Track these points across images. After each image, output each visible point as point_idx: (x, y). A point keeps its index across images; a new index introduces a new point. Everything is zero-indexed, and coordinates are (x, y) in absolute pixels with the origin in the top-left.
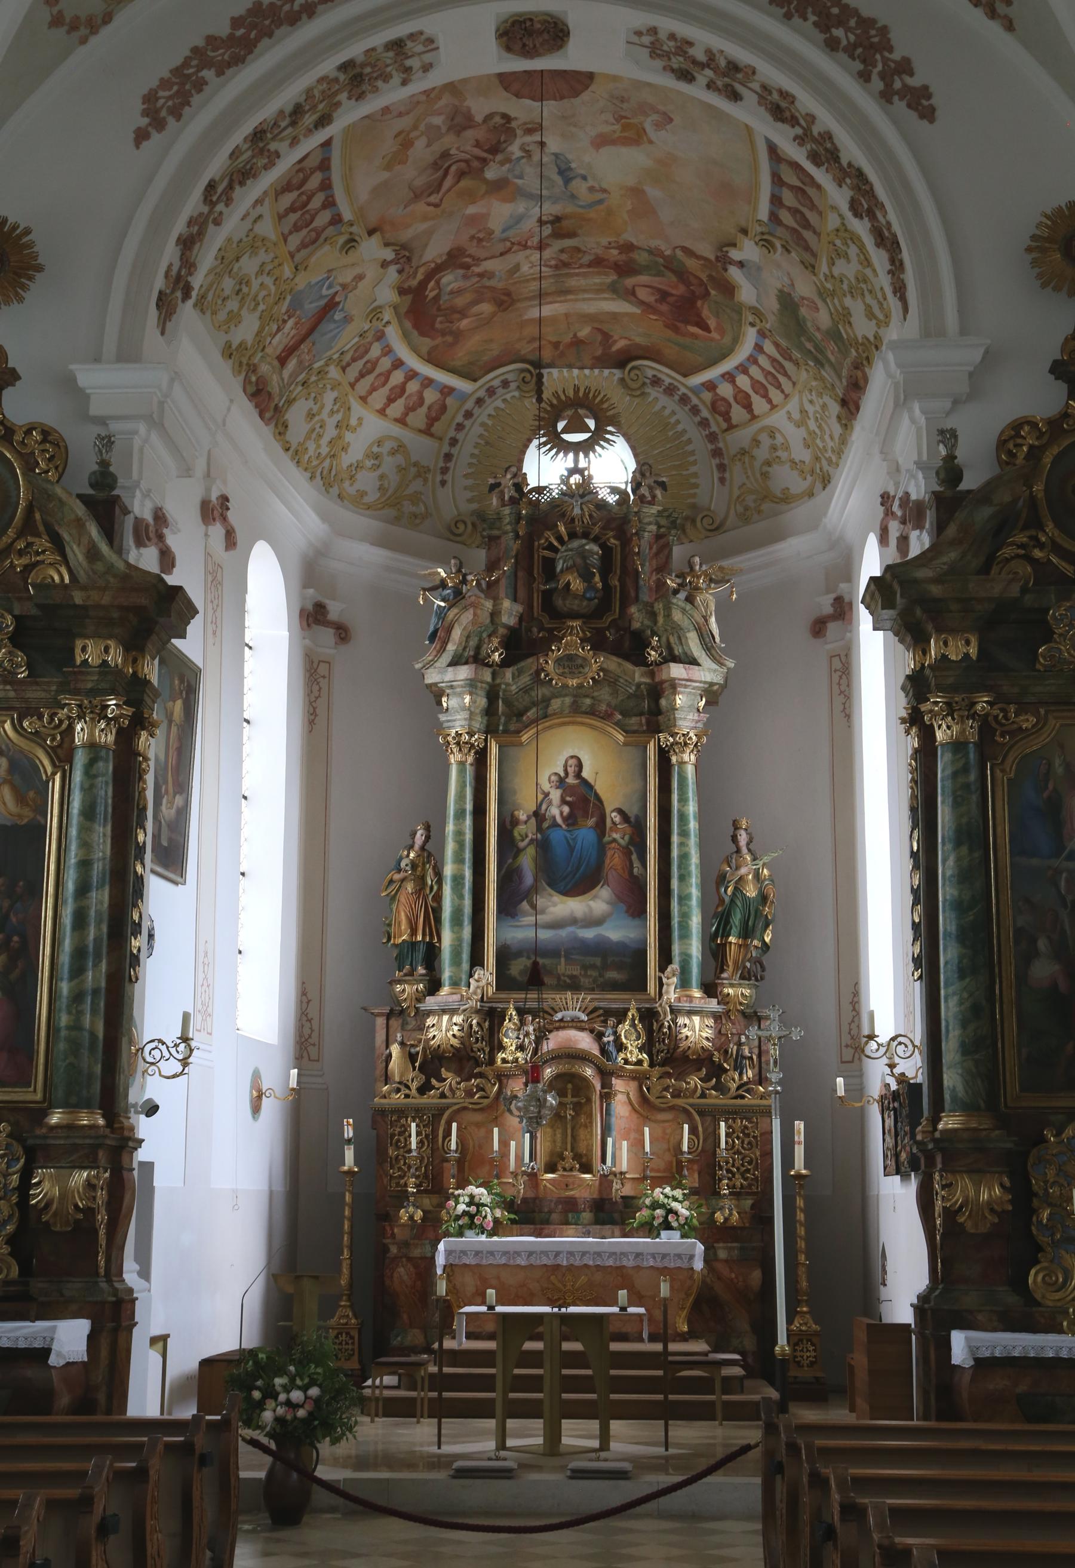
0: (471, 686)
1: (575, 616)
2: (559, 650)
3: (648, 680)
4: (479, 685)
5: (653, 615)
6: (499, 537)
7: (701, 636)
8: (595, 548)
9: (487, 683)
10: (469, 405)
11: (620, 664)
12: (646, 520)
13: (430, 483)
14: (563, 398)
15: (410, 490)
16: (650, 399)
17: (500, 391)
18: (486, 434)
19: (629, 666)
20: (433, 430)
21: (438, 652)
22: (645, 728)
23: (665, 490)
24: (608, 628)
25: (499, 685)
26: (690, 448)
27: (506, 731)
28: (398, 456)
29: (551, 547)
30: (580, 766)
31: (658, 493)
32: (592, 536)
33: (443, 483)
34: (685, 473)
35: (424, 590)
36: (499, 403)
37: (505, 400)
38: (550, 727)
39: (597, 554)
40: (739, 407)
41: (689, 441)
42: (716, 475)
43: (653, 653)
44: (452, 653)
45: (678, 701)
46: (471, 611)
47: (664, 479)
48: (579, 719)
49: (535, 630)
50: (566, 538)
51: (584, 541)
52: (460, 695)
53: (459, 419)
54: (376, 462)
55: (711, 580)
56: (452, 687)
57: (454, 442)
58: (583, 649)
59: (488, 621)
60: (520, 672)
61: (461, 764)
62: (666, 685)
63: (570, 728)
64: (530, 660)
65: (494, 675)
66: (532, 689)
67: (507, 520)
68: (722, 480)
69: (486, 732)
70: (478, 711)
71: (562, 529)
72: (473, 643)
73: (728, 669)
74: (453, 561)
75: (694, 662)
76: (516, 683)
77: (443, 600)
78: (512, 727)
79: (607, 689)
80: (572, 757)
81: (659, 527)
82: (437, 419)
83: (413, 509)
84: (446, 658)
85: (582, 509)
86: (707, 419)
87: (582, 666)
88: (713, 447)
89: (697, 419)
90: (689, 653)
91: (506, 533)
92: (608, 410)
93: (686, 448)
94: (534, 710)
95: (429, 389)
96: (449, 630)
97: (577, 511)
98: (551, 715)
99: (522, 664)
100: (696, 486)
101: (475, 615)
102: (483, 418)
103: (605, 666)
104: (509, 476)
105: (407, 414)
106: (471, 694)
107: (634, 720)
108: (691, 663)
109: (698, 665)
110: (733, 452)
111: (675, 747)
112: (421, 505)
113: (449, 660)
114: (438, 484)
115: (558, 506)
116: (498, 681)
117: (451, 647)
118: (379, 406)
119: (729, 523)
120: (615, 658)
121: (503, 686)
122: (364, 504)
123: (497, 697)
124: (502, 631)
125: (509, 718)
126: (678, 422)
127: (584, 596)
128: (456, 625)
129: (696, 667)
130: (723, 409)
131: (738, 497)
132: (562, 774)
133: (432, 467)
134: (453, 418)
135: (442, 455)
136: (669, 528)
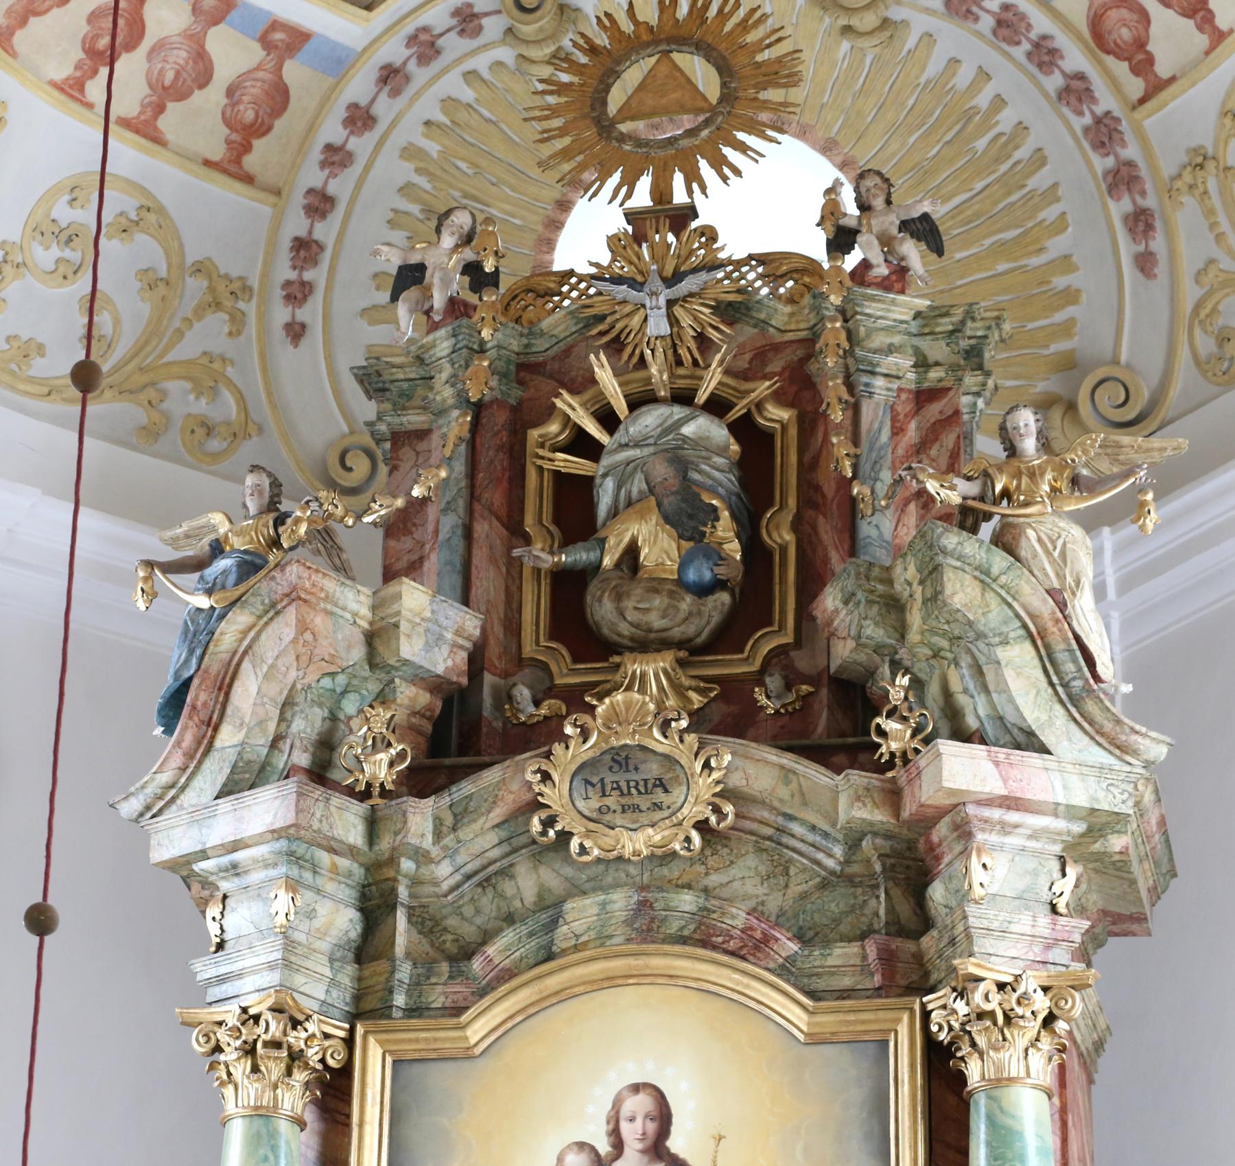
0: (292, 857)
1: (646, 644)
2: (585, 734)
3: (878, 816)
4: (324, 858)
5: (894, 607)
6: (422, 434)
7: (1048, 659)
8: (715, 431)
9: (352, 852)
10: (359, 87)
11: (786, 772)
12: (879, 340)
13: (252, 328)
14: (627, 26)
15: (188, 349)
16: (911, 43)
17: (453, 45)
18: (422, 182)
19: (814, 774)
20: (251, 162)
21: (190, 756)
22: (877, 980)
23: (938, 249)
24: (758, 678)
25: (392, 861)
26: (1042, 180)
27: (415, 1011)
28: (141, 238)
29: (582, 445)
30: (663, 1117)
31: (912, 251)
32: (702, 397)
33: (296, 332)
34: (1035, 261)
35: (150, 564)
36: (453, 85)
37: (471, 76)
38: (562, 996)
39: (722, 451)
40: (1170, 13)
41: (1039, 159)
42: (1127, 249)
43: (891, 726)
44: (232, 755)
45: (977, 874)
46: (291, 614)
47: (926, 207)
48: (658, 963)
49: (523, 693)
50: (621, 407)
51: (678, 412)
52: (259, 893)
53: (332, 130)
54: (67, 254)
55: (1075, 481)
56: (234, 870)
57: (320, 204)
58: (665, 727)
59: (358, 653)
60: (461, 815)
61: (262, 1115)
62: (942, 830)
63: (628, 995)
64: (492, 775)
65: (373, 825)
66: (506, 872)
67: (444, 376)
68: (1145, 262)
69: (353, 1018)
70: (324, 946)
71: (605, 375)
72: (308, 724)
73: (1147, 765)
74: (250, 480)
75: (1029, 741)
76: (450, 854)
77: (209, 592)
78: (437, 997)
79: (751, 861)
80: (636, 1088)
81: (922, 364)
82: (260, 129)
83: (201, 406)
84: (214, 772)
85: (673, 321)
86: (1081, 77)
87: (661, 784)
88: (1110, 162)
89: (1054, 82)
90: (1010, 717)
91: (442, 412)
92: (761, 46)
93: (1032, 183)
94: (508, 937)
95: (222, 28)
96: (225, 686)
97: (658, 326)
98: (564, 952)
99: (466, 788)
100: (1070, 296)
101: (303, 627)
102: (410, 132)
103: (736, 781)
104: (448, 241)
105: (160, 109)
106: (293, 886)
107: (842, 954)
108: (1018, 747)
109: (1044, 750)
110: (1167, 168)
111: (974, 1028)
112: (228, 397)
113: (221, 779)
114: (278, 333)
115: (601, 318)
116: (385, 844)
117: (228, 737)
118: (62, 71)
119: (1174, 392)
120: (773, 756)
121: (407, 865)
122: (31, 380)
123: (390, 905)
124: (409, 695)
125: (425, 968)
126: (999, 102)
127: (680, 582)
128: (246, 665)
129: (1033, 758)
130: (1126, 34)
131: (1198, 306)
132: (604, 1147)
133: (255, 282)
134: (312, 128)
135: (286, 243)
136: (954, 368)
